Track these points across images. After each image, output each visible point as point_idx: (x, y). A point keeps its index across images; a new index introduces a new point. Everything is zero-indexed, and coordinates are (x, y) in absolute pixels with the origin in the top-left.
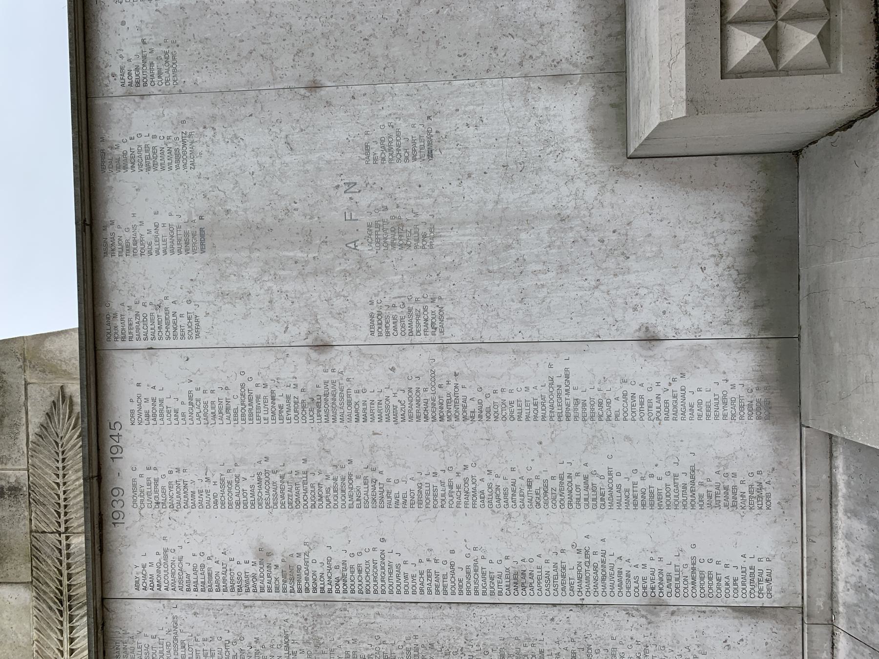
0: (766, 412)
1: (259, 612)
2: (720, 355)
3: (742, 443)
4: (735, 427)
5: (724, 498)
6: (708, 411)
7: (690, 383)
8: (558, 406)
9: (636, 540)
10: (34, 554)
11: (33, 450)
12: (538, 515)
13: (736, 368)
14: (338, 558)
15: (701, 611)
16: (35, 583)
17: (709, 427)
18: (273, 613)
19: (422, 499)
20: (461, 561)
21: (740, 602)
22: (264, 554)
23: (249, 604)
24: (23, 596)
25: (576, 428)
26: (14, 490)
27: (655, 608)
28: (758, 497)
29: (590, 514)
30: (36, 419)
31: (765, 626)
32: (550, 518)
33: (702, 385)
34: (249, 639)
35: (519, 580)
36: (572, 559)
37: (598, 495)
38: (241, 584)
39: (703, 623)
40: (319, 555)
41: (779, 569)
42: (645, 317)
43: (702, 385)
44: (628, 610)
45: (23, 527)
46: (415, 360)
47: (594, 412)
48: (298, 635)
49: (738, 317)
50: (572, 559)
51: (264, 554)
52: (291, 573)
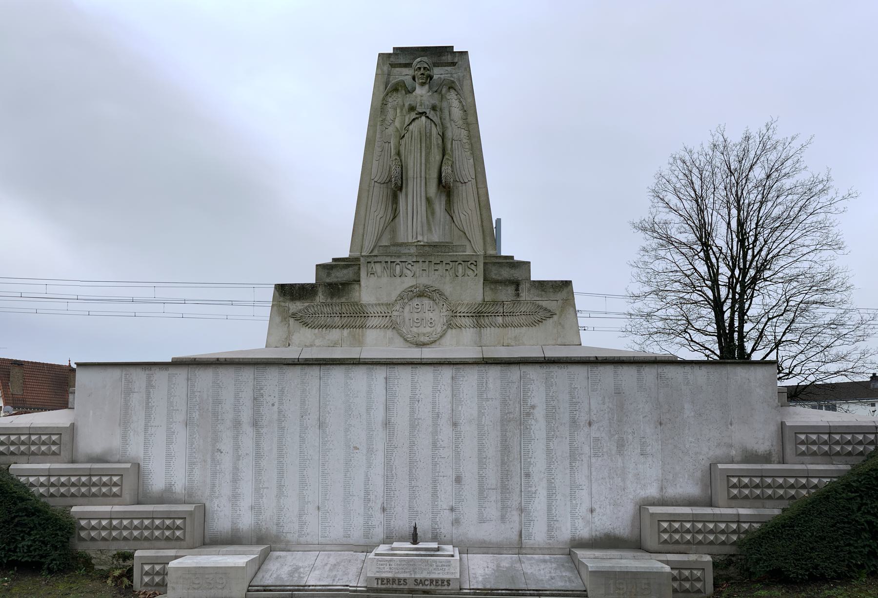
0: (573, 540)
1: (517, 405)
2: (588, 528)
3: (565, 533)
4: (569, 532)
5: (550, 529)
6: (573, 525)
7: (580, 521)
8: (574, 487)
9: (539, 505)
10: (495, 303)
11: (533, 303)
12: (545, 481)
13: (584, 532)
14: (533, 427)
15: (520, 522)
16: (484, 303)
17: (569, 525)
18: (517, 409)
19: (549, 451)
20: (532, 460)
21: (523, 532)
22: (533, 407)
23: (520, 402)
24: (479, 299)
25: (568, 491)
26: (518, 295)
27: (521, 510)
28: (551, 537)
29: (546, 494)
30: (544, 304)
31: (517, 538)
32: (544, 483)
33: (580, 524)
34: (511, 402)
35: (528, 475)
36: (533, 489)
37: (551, 496)
38: (525, 401)
39: (517, 522)
40: (533, 422)
41: (532, 542)
42: (598, 510)
43: (580, 524)
44: (521, 503)
45: (504, 298)
46: (586, 449)
47: (572, 496)
48: (511, 416)
49: (598, 533)
50: (533, 489)
51: (533, 407)
52: (528, 414)
